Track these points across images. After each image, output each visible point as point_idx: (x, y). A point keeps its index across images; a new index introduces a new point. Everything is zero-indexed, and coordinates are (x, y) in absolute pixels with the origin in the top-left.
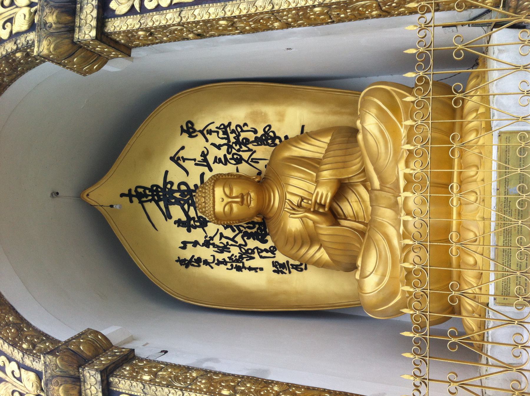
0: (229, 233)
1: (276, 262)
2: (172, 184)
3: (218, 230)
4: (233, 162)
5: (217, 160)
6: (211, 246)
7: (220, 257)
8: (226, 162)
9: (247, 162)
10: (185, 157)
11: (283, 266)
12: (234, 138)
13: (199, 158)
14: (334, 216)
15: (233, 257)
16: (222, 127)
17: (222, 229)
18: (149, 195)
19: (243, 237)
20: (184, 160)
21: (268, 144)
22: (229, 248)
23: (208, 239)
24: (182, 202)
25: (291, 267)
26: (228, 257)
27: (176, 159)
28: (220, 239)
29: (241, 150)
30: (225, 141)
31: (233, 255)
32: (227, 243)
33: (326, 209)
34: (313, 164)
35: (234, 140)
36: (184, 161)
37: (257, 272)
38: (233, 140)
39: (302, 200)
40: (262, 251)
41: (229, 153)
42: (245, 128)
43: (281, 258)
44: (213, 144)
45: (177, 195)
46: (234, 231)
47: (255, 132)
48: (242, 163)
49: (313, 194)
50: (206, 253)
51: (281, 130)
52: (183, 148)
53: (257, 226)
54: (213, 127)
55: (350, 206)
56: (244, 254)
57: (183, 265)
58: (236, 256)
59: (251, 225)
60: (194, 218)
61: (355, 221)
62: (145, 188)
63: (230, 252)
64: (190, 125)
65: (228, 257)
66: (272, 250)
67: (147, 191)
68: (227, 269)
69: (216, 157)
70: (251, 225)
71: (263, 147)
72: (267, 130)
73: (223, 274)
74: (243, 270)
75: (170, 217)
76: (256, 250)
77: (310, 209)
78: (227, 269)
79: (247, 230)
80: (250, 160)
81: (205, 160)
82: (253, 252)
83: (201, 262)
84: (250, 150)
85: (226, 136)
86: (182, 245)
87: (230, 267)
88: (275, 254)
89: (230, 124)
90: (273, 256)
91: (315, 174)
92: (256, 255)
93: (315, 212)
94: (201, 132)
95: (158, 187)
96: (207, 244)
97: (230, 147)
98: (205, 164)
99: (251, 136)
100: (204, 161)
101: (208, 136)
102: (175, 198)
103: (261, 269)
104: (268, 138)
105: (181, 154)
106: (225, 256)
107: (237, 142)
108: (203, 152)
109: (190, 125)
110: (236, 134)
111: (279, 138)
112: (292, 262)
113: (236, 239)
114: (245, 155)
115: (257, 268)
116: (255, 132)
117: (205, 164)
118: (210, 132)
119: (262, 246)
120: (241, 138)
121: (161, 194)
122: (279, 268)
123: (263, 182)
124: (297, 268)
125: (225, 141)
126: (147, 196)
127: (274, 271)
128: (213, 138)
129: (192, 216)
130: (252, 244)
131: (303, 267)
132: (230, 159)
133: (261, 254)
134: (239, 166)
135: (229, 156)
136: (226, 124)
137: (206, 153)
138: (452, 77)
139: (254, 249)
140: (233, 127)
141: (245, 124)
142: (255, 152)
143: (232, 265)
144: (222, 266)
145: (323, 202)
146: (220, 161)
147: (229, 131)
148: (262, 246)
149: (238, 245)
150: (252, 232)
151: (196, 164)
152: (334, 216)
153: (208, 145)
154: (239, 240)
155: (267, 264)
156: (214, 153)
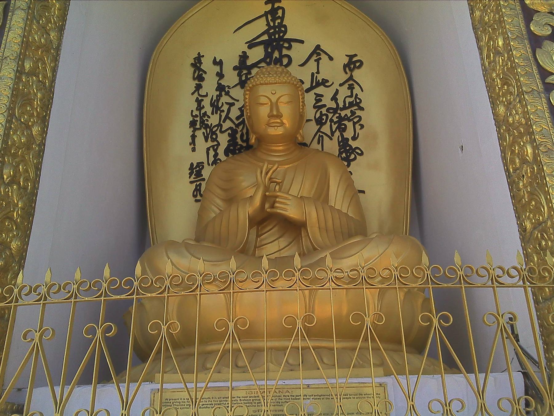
0: (234, 113)
1: (203, 167)
2: (289, 48)
3: (238, 101)
4: (318, 115)
5: (319, 97)
6: (218, 93)
7: (206, 103)
8: (317, 107)
9: (319, 131)
10: (320, 61)
11: (199, 174)
12: (346, 115)
13: (320, 78)
15: (206, 118)
16: (358, 101)
17: (238, 105)
18: (274, 23)
19: (231, 128)
20: (318, 61)
21: (340, 153)
22: (216, 113)
23: (227, 89)
24: (268, 60)
25: (198, 183)
26: (206, 112)
27: (318, 51)
28: (227, 103)
29: (333, 124)
30: (341, 105)
31: (209, 117)
32: (223, 111)
33: (268, 210)
34: (321, 196)
35: (343, 115)
36: (315, 60)
37: (190, 144)
38: (343, 113)
39: (278, 183)
40: (215, 151)
41: (328, 110)
42: (358, 127)
44: (337, 92)
45: (276, 54)
46: (238, 118)
47: (354, 138)
48: (317, 125)
49: (288, 193)
50: (210, 86)
51: (358, 168)
52: (331, 59)
53: (244, 145)
54: (357, 90)
55: (274, 245)
56: (211, 130)
57: (195, 61)
58: (208, 121)
59: (245, 138)
60: (250, 73)
61: (255, 247)
62: (282, 18)
63: (212, 114)
64: (358, 64)
65: (206, 112)
67: (279, 21)
68: (192, 111)
69: (322, 96)
70: (245, 138)
71: (338, 148)
72: (357, 151)
73: (186, 105)
74: (192, 129)
75: (250, 47)
76: (216, 143)
77: (267, 191)
78: (192, 111)
79: (239, 133)
80: (321, 134)
81: (318, 84)
82: (213, 140)
83: (199, 81)
84: (333, 133)
85: (347, 105)
86: (218, 60)
87: (194, 114)
88: (212, 165)
89: (362, 109)
90: (210, 163)
91: (311, 196)
92: (210, 144)
93: (265, 198)
94: (351, 78)
95: (285, 32)
96: (221, 88)
97: (335, 111)
98: (314, 84)
99: (349, 134)
101: (346, 86)
102: (273, 52)
103: (194, 150)
104: (348, 153)
105: (324, 57)
106: (208, 109)
107: (341, 119)
108: (327, 81)
109: (358, 64)
110: (351, 116)
111: (349, 165)
112: (204, 184)
113: (228, 121)
114: (326, 129)
115: (194, 145)
116: (354, 138)
117: (314, 84)
118: (351, 88)
119: (221, 151)
120: (346, 122)
121: (277, 36)
122: (196, 171)
124: (198, 189)
125: (341, 105)
126: (274, 20)
127: (192, 164)
128: (344, 92)
129: (252, 71)
130: (224, 139)
131: (199, 198)
132: (321, 112)
133: (211, 149)
134: (314, 122)
135: (324, 111)
136: (361, 105)
137: (326, 84)
138: (444, 335)
139: (218, 141)
140: (358, 113)
141: (362, 126)
142: (331, 139)
143: (196, 116)
144: (196, 105)
145: (277, 205)
146: (318, 101)
147: (353, 109)
148: (221, 151)
149: (221, 123)
150: (237, 138)
151: (313, 74)
153: (336, 86)
154: (227, 125)
155: (200, 156)
156: (327, 93)
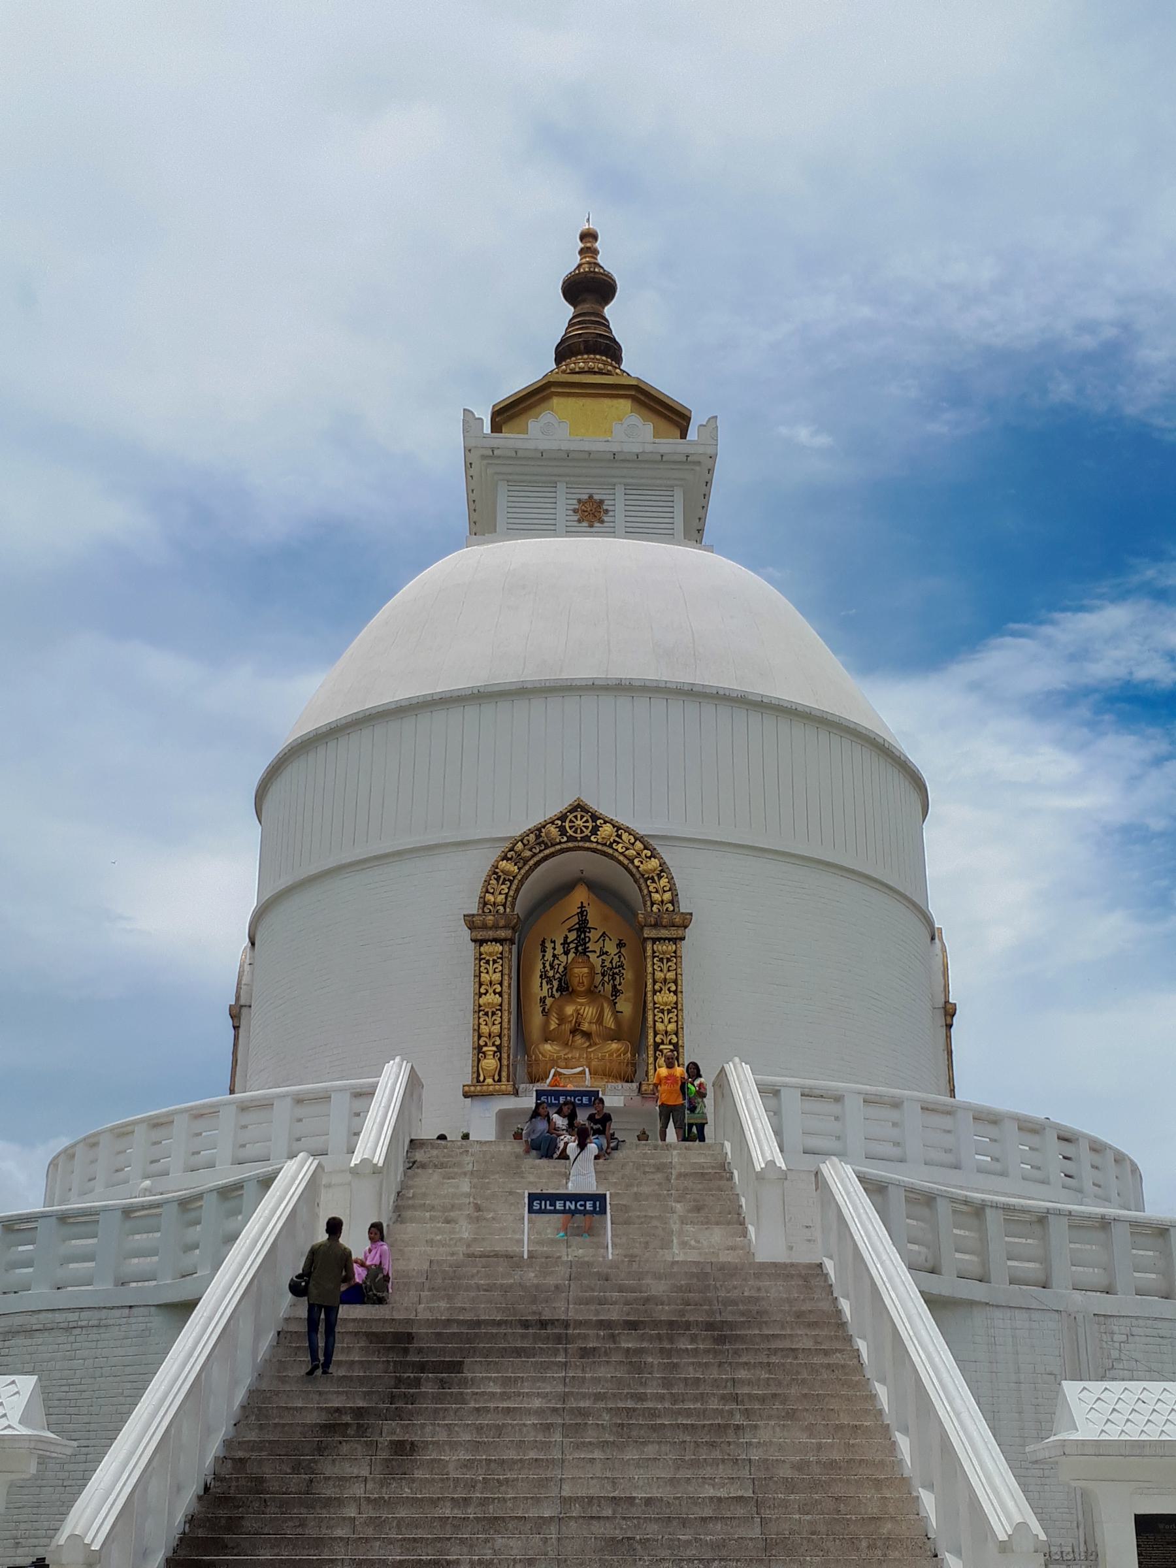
0: (561, 969)
7: (547, 964)
14: (574, 1031)
34: (600, 1020)
43: (549, 1001)
50: (549, 956)
55: (579, 1040)
66: (552, 996)
96: (554, 956)
99: (617, 982)
100: (603, 953)
104: (616, 992)
106: (548, 968)
114: (606, 979)
123: (592, 993)
130: (555, 983)
152: (574, 1031)
154: (557, 976)
155: (545, 993)
